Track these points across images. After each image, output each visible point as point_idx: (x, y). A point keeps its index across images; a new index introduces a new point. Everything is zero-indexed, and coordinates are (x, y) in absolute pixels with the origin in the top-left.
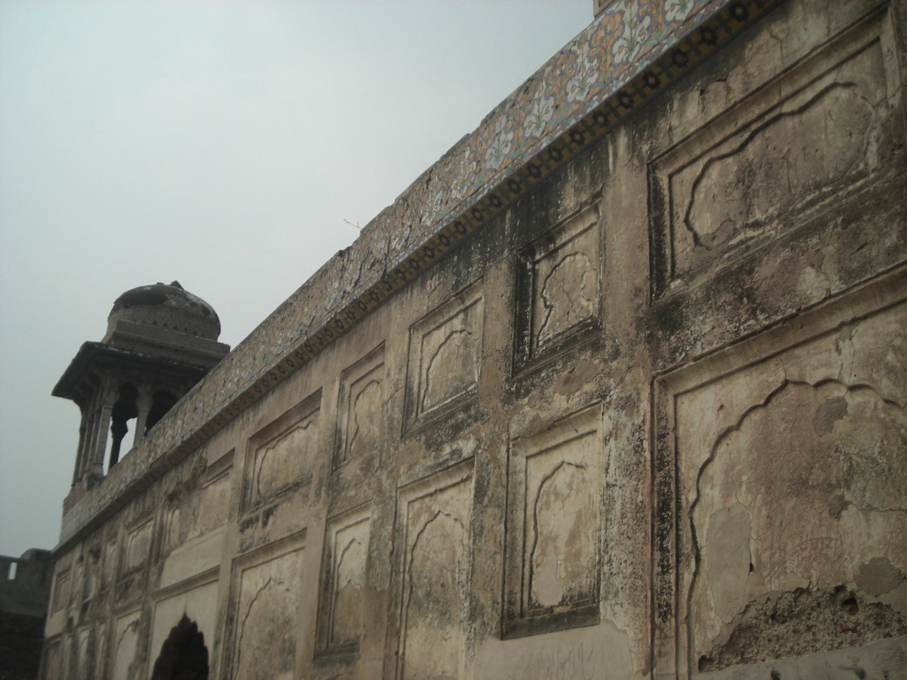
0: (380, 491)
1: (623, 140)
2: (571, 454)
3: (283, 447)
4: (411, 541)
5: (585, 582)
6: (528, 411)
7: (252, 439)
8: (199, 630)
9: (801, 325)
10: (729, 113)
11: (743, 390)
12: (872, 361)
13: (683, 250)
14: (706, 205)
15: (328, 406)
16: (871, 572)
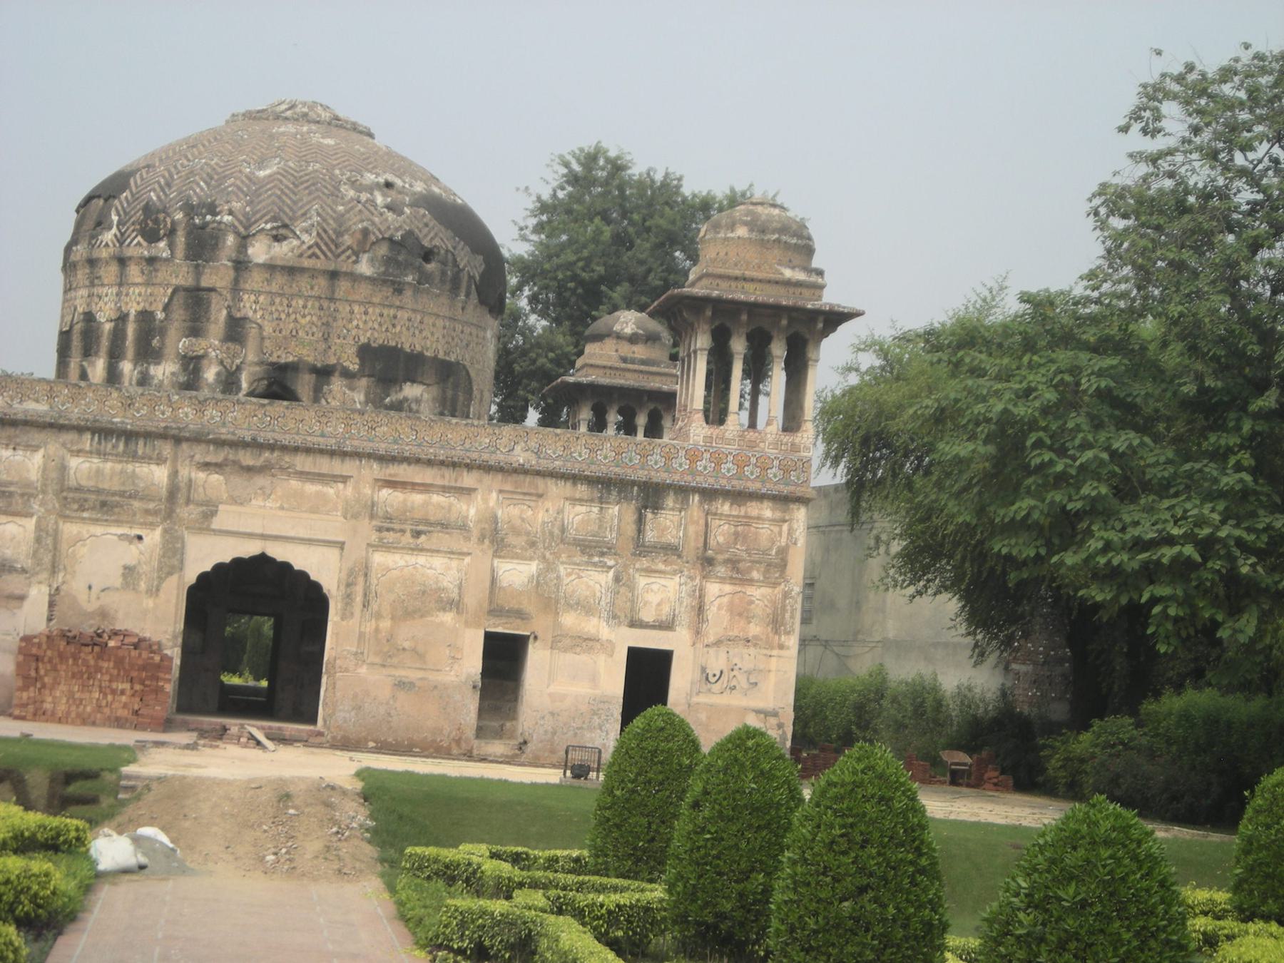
0: (544, 557)
1: (697, 498)
2: (663, 581)
3: (417, 498)
4: (565, 582)
5: (664, 618)
6: (645, 563)
7: (377, 480)
8: (296, 568)
9: (751, 582)
10: (738, 516)
11: (728, 588)
12: (763, 595)
13: (712, 543)
14: (721, 533)
15: (486, 501)
16: (756, 637)
